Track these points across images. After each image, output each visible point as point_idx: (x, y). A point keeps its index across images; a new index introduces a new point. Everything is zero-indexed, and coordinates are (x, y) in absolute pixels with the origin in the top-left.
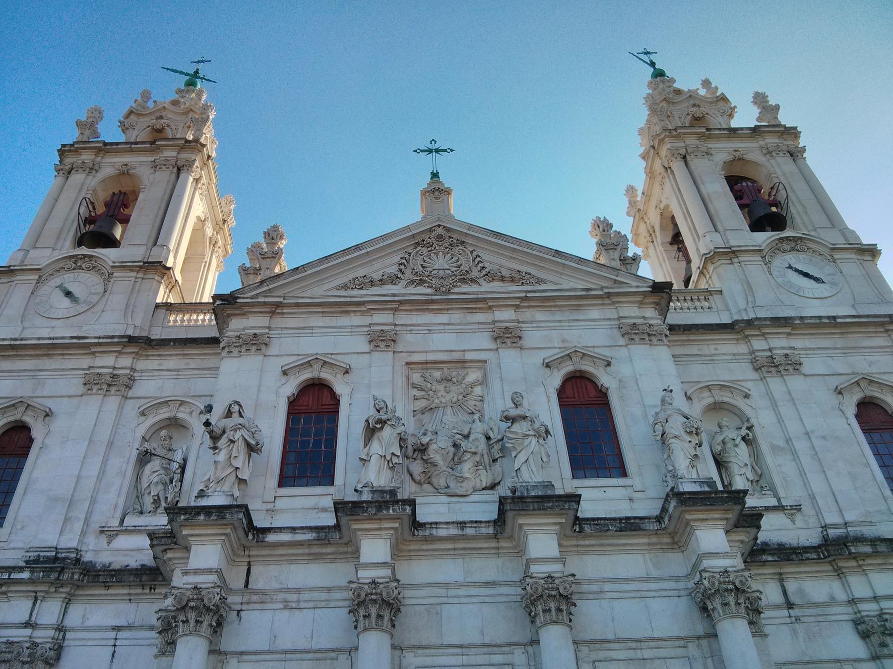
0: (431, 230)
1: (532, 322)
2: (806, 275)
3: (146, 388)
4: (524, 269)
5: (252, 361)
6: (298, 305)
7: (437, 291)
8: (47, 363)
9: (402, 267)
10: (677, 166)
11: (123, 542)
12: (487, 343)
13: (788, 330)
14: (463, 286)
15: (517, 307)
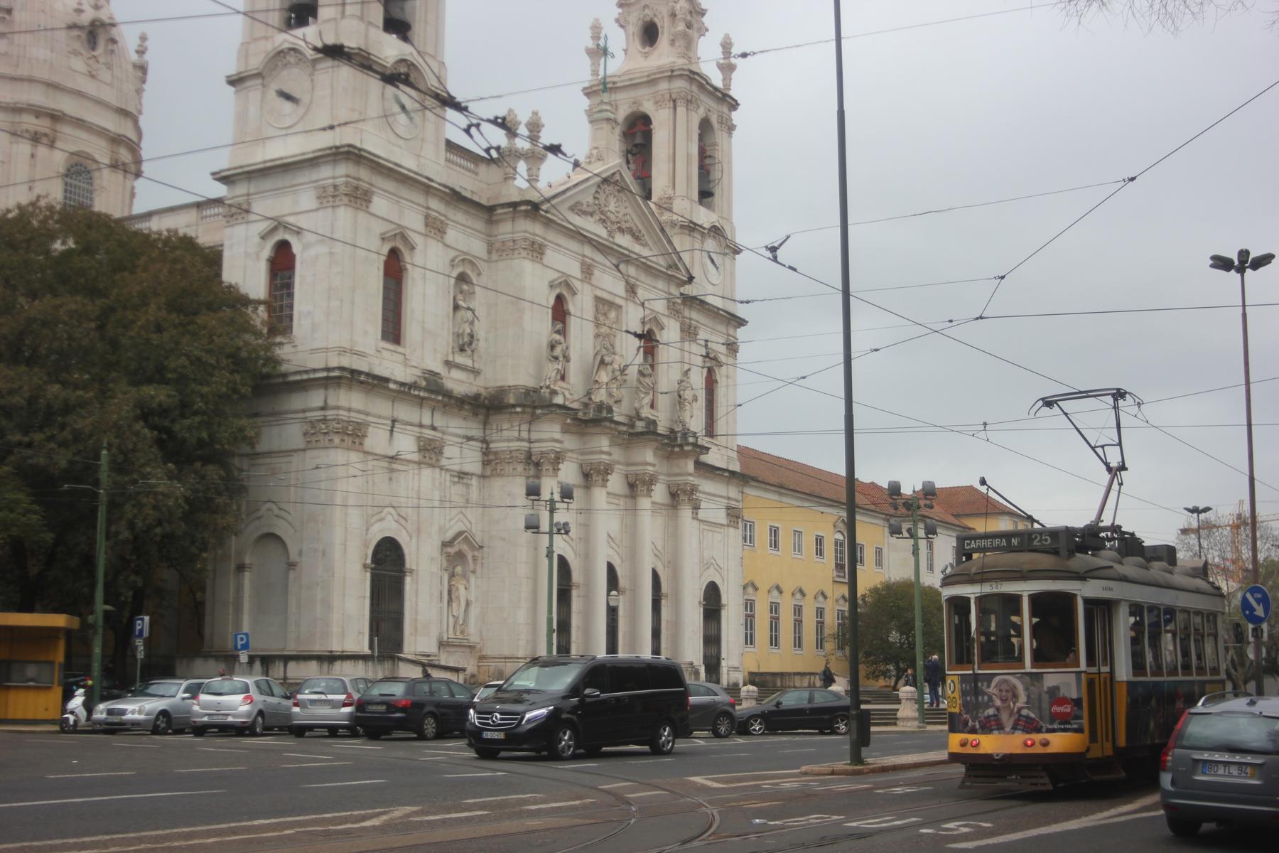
0: (614, 174)
1: (640, 281)
2: (712, 261)
3: (452, 235)
4: (644, 232)
5: (538, 266)
6: (560, 225)
7: (610, 235)
8: (405, 192)
9: (597, 202)
10: (681, 110)
11: (456, 374)
12: (623, 294)
13: (698, 307)
14: (618, 233)
15: (637, 266)
